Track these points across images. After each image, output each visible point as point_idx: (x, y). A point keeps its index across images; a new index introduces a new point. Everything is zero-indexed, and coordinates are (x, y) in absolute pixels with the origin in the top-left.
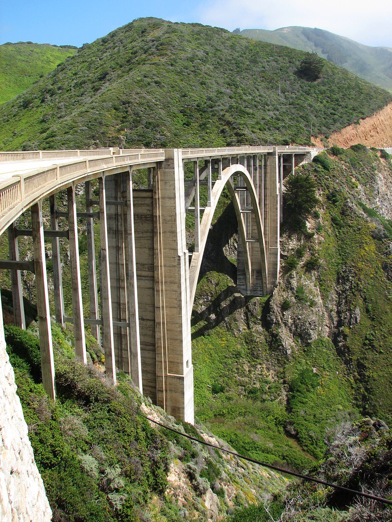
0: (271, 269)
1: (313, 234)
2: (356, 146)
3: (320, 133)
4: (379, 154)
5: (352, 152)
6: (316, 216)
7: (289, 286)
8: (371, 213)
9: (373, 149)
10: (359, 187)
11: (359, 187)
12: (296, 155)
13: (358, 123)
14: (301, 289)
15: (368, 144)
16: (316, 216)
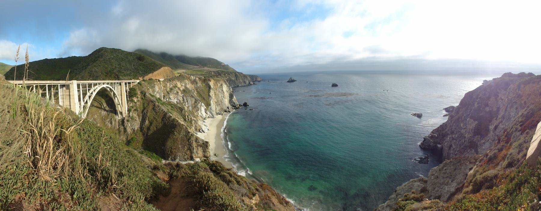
0: (125, 112)
1: (137, 102)
2: (150, 79)
3: (142, 76)
4: (157, 81)
5: (149, 81)
6: (138, 98)
7: (129, 116)
8: (152, 96)
9: (156, 79)
10: (150, 90)
11: (150, 89)
12: (132, 82)
13: (153, 73)
14: (132, 116)
15: (154, 78)
16: (138, 98)
